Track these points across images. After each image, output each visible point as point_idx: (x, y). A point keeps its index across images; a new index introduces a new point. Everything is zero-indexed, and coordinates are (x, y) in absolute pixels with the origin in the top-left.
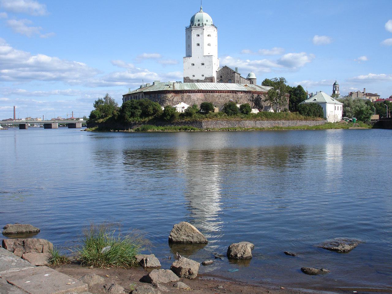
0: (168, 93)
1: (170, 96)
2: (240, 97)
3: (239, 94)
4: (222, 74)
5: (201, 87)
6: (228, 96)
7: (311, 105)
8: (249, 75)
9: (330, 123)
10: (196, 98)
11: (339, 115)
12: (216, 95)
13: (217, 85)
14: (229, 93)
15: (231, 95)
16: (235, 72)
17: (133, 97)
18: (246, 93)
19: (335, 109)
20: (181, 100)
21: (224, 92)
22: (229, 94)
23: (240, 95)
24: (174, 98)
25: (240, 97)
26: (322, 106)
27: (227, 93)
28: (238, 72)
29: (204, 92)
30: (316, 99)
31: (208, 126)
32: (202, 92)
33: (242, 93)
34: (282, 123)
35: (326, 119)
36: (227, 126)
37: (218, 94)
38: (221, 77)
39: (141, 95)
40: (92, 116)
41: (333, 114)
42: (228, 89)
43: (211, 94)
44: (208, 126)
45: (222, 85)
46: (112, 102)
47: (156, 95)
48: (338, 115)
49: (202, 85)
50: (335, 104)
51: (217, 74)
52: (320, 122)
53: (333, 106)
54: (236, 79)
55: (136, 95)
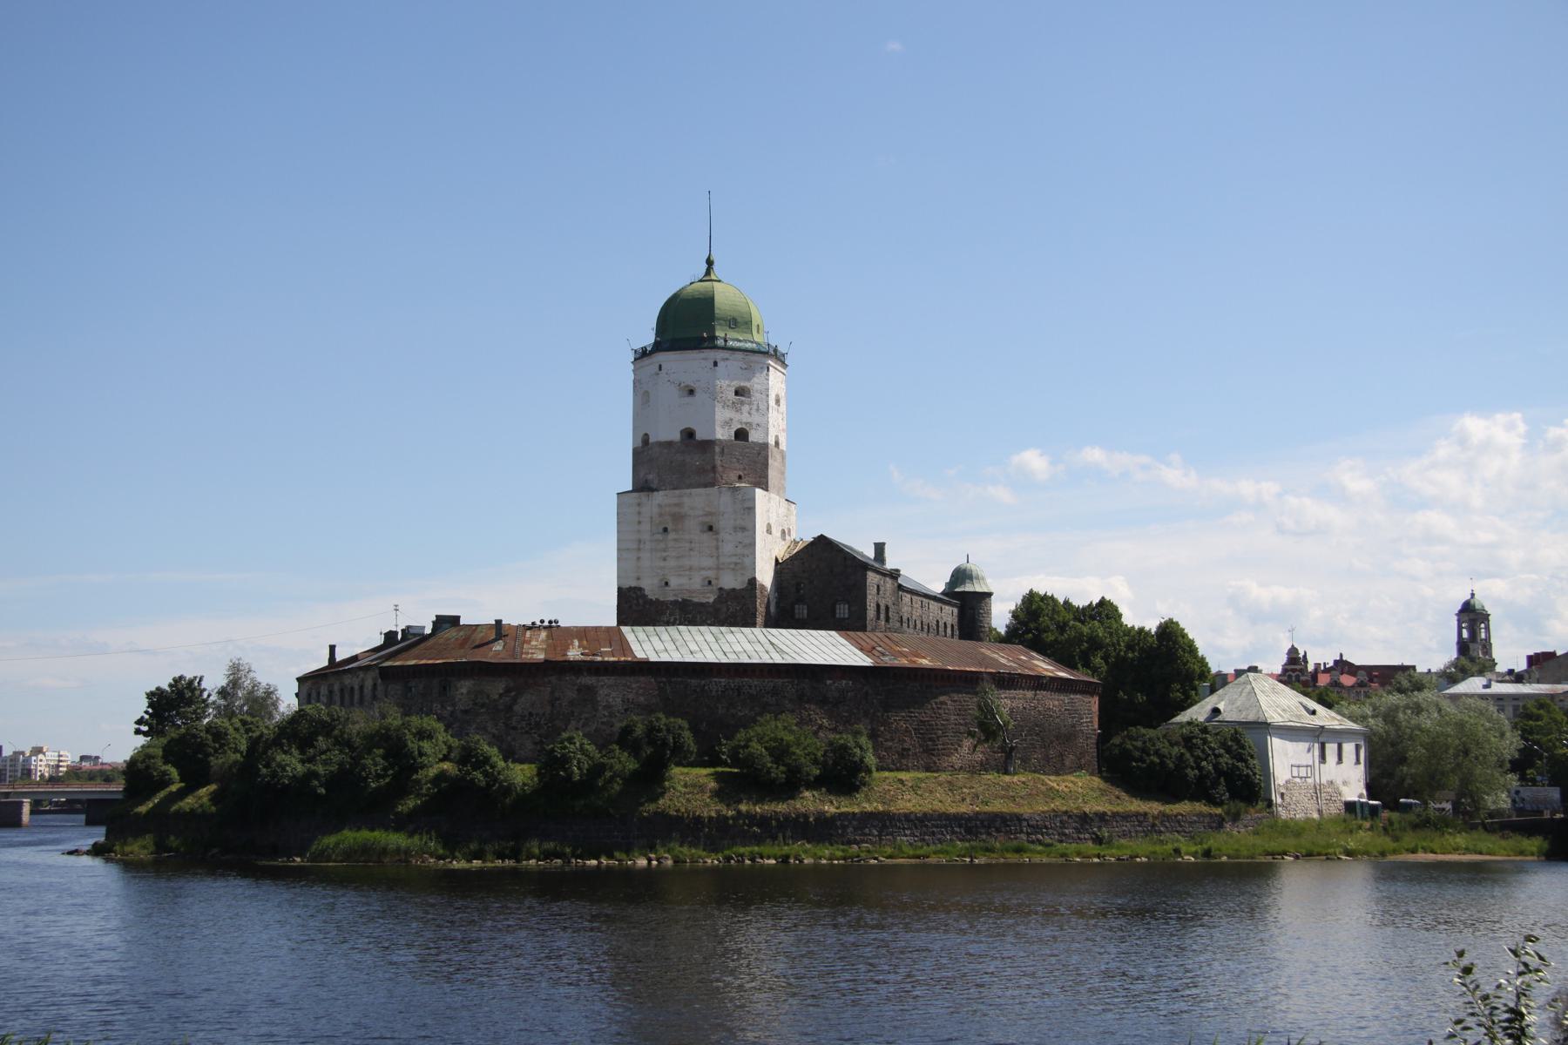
1: (496, 688)
5: (647, 646)
7: (1193, 737)
8: (960, 575)
9: (1295, 829)
13: (730, 637)
17: (336, 688)
22: (779, 681)
24: (515, 701)
28: (890, 565)
30: (1221, 706)
35: (1270, 804)
39: (369, 684)
40: (138, 774)
42: (778, 659)
43: (694, 682)
45: (751, 637)
46: (275, 705)
48: (1339, 782)
49: (655, 639)
55: (347, 680)
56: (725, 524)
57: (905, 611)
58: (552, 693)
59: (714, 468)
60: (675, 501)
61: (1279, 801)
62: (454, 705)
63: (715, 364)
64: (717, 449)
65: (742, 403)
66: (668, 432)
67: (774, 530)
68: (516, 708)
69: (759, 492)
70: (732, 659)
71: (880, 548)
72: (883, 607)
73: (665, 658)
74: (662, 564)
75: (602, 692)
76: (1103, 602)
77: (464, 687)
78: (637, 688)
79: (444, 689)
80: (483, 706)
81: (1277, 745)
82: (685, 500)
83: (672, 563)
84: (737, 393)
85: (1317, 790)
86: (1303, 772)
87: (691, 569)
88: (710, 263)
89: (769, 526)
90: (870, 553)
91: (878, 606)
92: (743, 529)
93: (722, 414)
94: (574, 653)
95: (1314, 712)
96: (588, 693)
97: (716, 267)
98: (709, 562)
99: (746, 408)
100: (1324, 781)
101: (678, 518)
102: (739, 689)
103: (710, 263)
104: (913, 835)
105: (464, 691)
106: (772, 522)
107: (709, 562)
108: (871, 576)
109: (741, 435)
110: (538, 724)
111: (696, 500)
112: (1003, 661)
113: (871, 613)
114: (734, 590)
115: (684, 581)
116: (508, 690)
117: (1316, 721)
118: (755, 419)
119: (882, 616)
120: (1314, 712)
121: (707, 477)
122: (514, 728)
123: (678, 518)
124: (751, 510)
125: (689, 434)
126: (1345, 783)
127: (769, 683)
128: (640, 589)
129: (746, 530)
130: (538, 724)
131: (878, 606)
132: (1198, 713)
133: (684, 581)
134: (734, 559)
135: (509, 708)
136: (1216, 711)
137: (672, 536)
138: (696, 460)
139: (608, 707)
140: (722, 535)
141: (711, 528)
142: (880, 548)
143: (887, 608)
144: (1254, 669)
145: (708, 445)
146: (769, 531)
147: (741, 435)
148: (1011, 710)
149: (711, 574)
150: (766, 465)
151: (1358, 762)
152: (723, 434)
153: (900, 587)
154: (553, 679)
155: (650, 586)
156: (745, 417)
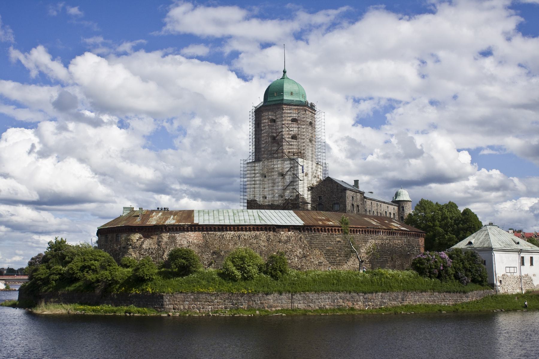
1: (136, 237)
2: (284, 238)
3: (282, 233)
4: (322, 193)
6: (256, 237)
9: (506, 297)
11: (534, 275)
12: (229, 234)
14: (258, 231)
15: (263, 235)
16: (345, 189)
18: (300, 231)
19: (523, 264)
20: (157, 246)
21: (246, 228)
22: (258, 233)
23: (284, 235)
24: (143, 243)
25: (284, 238)
26: (482, 256)
29: (203, 230)
30: (473, 241)
31: (176, 304)
32: (199, 230)
33: (289, 231)
35: (492, 286)
36: (220, 306)
41: (517, 274)
43: (219, 233)
44: (176, 304)
47: (115, 235)
48: (531, 275)
50: (521, 251)
52: (474, 296)
53: (515, 257)
54: (349, 202)
57: (368, 207)
61: (498, 284)
62: (120, 245)
68: (144, 246)
69: (300, 160)
70: (237, 223)
71: (356, 182)
72: (355, 205)
73: (206, 223)
75: (179, 238)
76: (450, 202)
77: (123, 237)
79: (117, 236)
80: (131, 245)
81: (498, 257)
86: (512, 270)
88: (285, 72)
91: (353, 205)
94: (171, 221)
95: (518, 243)
100: (523, 274)
102: (239, 236)
103: (285, 72)
104: (304, 303)
105: (123, 239)
108: (348, 192)
112: (374, 223)
113: (349, 207)
116: (140, 238)
117: (519, 247)
119: (355, 209)
120: (518, 243)
122: (142, 255)
126: (534, 275)
127: (253, 233)
130: (152, 253)
131: (353, 205)
132: (462, 245)
136: (470, 243)
142: (356, 182)
143: (358, 206)
144: (491, 224)
153: (365, 197)
155: (259, 199)
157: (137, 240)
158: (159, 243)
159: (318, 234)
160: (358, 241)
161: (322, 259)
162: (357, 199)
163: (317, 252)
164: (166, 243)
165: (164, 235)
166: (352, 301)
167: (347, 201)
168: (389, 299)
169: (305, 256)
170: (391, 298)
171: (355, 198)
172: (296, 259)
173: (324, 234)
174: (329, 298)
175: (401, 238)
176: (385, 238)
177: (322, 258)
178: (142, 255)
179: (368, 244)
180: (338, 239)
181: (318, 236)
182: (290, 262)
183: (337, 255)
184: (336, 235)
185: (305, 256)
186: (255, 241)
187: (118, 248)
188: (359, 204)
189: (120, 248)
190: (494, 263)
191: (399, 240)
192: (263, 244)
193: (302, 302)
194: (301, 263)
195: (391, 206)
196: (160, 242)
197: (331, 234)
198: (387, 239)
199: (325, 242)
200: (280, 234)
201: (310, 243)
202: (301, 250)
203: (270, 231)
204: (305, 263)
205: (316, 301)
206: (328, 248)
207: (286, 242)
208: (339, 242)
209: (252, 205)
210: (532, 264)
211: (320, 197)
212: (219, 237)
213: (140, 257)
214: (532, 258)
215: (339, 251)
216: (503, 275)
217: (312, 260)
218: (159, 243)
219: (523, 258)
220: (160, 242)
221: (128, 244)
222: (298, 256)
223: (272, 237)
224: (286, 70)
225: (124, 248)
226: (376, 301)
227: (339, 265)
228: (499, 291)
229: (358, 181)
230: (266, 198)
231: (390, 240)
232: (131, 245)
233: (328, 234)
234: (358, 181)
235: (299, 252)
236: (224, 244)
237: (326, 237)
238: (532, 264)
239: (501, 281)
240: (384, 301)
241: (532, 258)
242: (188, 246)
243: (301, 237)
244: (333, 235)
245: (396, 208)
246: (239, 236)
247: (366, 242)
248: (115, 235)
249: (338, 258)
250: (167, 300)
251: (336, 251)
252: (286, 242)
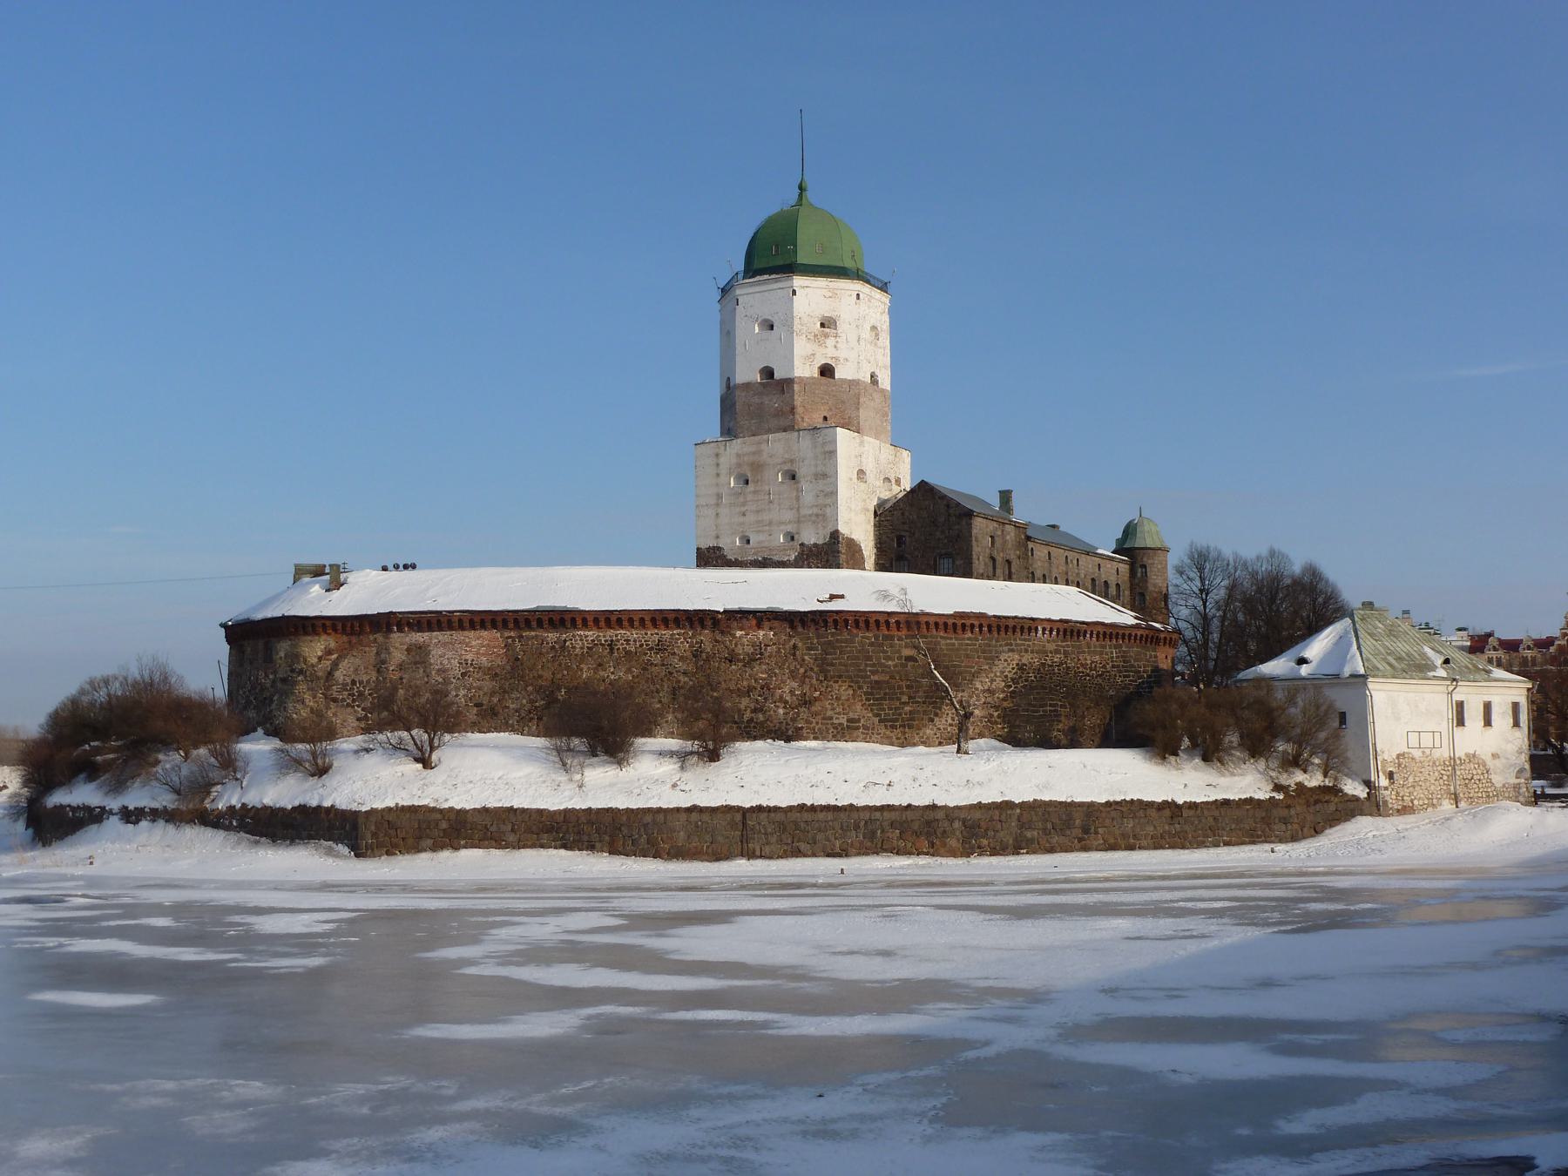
0: (306, 633)
1: (314, 649)
3: (739, 633)
6: (660, 647)
8: (1130, 530)
10: (455, 662)
11: (1495, 756)
14: (667, 627)
16: (969, 514)
18: (793, 627)
19: (1461, 722)
20: (374, 675)
22: (666, 633)
24: (335, 665)
26: (1340, 698)
27: (655, 626)
29: (505, 625)
33: (759, 626)
34: (957, 824)
37: (591, 634)
38: (900, 539)
41: (1443, 753)
43: (552, 636)
47: (261, 644)
48: (1485, 754)
51: (879, 526)
56: (803, 471)
58: (378, 654)
59: (793, 410)
60: (753, 449)
61: (1384, 782)
62: (275, 673)
63: (794, 292)
64: (796, 387)
65: (826, 336)
66: (747, 373)
67: (870, 476)
71: (1006, 497)
72: (999, 559)
74: (742, 519)
75: (436, 652)
77: (282, 648)
78: (480, 647)
80: (301, 672)
82: (764, 446)
83: (751, 518)
84: (822, 325)
85: (1453, 763)
87: (770, 523)
89: (861, 473)
90: (995, 503)
92: (825, 476)
93: (801, 347)
96: (419, 654)
97: (810, 195)
98: (788, 515)
99: (830, 342)
101: (758, 467)
102: (611, 645)
103: (801, 188)
105: (282, 654)
106: (869, 467)
107: (788, 515)
108: (978, 525)
109: (827, 371)
110: (361, 694)
111: (775, 446)
114: (815, 545)
115: (762, 537)
116: (329, 652)
118: (842, 354)
121: (786, 420)
122: (335, 700)
123: (758, 467)
124: (832, 454)
125: (768, 373)
127: (652, 635)
128: (719, 548)
129: (826, 476)
130: (361, 694)
131: (993, 559)
133: (762, 537)
134: (815, 510)
135: (330, 674)
136: (1302, 661)
137: (751, 487)
138: (773, 402)
139: (441, 671)
140: (805, 485)
141: (793, 477)
142: (1006, 497)
143: (1009, 562)
145: (789, 382)
146: (861, 473)
147: (827, 371)
148: (1021, 667)
149: (789, 528)
150: (857, 406)
151: (1516, 724)
152: (804, 369)
153: (1028, 538)
154: (380, 637)
155: (731, 544)
156: (831, 352)
157: (320, 658)
158: (380, 666)
159: (846, 636)
160: (967, 656)
161: (858, 710)
162: (1005, 542)
163: (844, 690)
164: (401, 667)
165: (396, 637)
166: (928, 834)
167: (976, 550)
168: (1044, 830)
169: (806, 702)
170: (1049, 826)
171: (998, 542)
172: (781, 711)
173: (863, 637)
174: (857, 827)
175: (1104, 647)
176: (1051, 647)
177: (859, 707)
178: (335, 700)
179: (1000, 666)
180: (907, 652)
181: (846, 641)
182: (761, 717)
183: (905, 699)
184: (900, 639)
185: (806, 702)
186: (657, 659)
187: (268, 683)
188: (1012, 557)
189: (274, 681)
190: (1370, 719)
191: (1095, 653)
192: (680, 665)
193: (773, 839)
194: (794, 720)
195: (1109, 564)
196: (383, 662)
197: (886, 637)
198: (1057, 651)
199: (869, 658)
200: (734, 636)
201: (823, 666)
202: (795, 685)
203: (703, 627)
204: (808, 722)
205: (820, 836)
206: (876, 678)
207: (751, 661)
208: (909, 659)
209: (709, 558)
210: (1488, 722)
211: (900, 538)
212: (553, 648)
213: (328, 708)
214: (1488, 707)
215: (908, 687)
216: (1398, 756)
217: (829, 713)
218: (380, 666)
219: (1460, 705)
220: (383, 662)
221: (293, 671)
222: (786, 702)
223: (708, 647)
224: (808, 184)
225: (284, 680)
226: (1002, 834)
227: (910, 727)
228: (1385, 802)
229: (1009, 492)
230: (748, 542)
231: (1066, 654)
232: (301, 672)
233: (876, 637)
234: (1009, 492)
235: (789, 688)
236: (568, 668)
237: (872, 644)
238: (1488, 722)
239: (1391, 776)
240: (1029, 834)
241: (1488, 707)
242: (463, 675)
243: (795, 647)
244: (891, 638)
245: (1124, 568)
246: (611, 645)
247: (992, 659)
248: (261, 644)
249: (907, 709)
250: (369, 835)
251: (900, 687)
252: (751, 661)
